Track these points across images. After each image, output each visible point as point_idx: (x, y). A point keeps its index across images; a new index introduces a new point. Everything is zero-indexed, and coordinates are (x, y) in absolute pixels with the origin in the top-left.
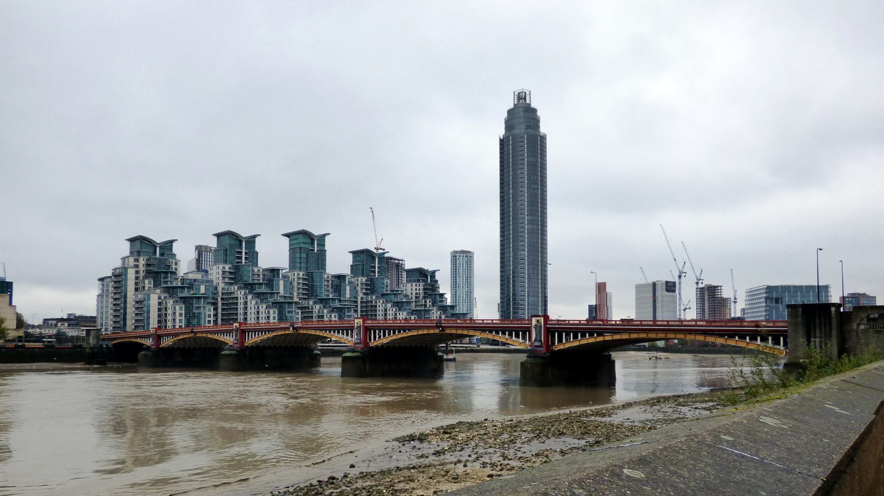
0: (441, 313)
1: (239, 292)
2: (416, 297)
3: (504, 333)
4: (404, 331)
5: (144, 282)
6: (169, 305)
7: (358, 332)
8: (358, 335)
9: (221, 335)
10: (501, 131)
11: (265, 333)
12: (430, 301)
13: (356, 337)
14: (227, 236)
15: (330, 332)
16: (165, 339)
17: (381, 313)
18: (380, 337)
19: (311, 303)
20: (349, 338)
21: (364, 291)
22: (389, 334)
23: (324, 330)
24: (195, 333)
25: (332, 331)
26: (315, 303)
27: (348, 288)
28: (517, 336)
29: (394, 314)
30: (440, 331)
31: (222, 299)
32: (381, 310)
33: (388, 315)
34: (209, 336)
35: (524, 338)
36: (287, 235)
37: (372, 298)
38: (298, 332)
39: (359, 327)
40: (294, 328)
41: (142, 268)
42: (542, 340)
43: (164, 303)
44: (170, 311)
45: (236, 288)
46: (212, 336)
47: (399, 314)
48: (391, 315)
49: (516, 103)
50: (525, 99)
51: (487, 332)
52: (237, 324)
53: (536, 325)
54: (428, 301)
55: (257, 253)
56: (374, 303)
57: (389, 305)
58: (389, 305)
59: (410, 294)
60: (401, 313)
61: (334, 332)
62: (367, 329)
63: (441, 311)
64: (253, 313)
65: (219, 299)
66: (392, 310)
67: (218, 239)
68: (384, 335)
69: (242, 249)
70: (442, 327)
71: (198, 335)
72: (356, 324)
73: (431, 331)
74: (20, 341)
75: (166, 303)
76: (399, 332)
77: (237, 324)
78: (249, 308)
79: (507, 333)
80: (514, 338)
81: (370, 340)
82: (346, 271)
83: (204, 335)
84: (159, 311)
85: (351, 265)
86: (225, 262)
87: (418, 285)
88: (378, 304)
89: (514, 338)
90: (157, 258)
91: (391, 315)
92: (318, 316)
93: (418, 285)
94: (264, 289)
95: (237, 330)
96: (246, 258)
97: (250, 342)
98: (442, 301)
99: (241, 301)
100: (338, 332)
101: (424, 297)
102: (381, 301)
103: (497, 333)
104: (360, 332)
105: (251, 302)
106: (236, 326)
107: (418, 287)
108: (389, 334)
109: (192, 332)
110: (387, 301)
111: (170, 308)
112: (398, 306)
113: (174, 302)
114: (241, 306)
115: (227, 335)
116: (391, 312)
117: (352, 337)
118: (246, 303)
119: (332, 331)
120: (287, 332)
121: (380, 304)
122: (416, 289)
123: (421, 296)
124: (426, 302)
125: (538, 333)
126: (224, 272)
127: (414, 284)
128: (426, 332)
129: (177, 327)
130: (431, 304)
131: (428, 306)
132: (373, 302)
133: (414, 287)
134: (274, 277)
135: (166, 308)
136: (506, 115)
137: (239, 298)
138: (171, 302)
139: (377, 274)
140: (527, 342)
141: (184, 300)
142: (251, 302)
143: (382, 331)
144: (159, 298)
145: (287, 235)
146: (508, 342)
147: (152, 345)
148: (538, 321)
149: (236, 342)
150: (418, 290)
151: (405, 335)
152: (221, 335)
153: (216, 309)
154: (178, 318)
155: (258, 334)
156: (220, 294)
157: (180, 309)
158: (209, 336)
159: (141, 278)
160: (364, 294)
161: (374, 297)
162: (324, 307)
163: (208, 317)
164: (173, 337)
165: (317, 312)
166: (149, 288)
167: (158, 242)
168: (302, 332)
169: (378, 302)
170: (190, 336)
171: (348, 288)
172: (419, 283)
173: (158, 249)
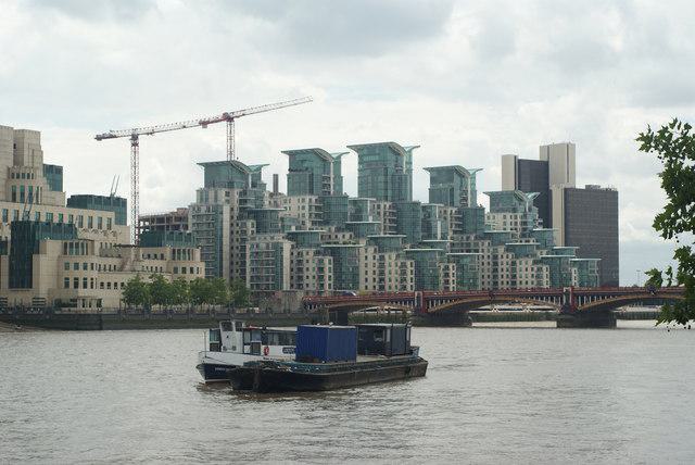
27: (439, 224)
37: (468, 238)
41: (236, 205)
57: (501, 250)
58: (501, 250)
64: (370, 265)
86: (311, 192)
101: (523, 236)
107: (513, 220)
116: (505, 259)
126: (310, 206)
127: (508, 215)
133: (508, 220)
138: (311, 254)
160: (455, 232)
166: (253, 232)
171: (439, 224)
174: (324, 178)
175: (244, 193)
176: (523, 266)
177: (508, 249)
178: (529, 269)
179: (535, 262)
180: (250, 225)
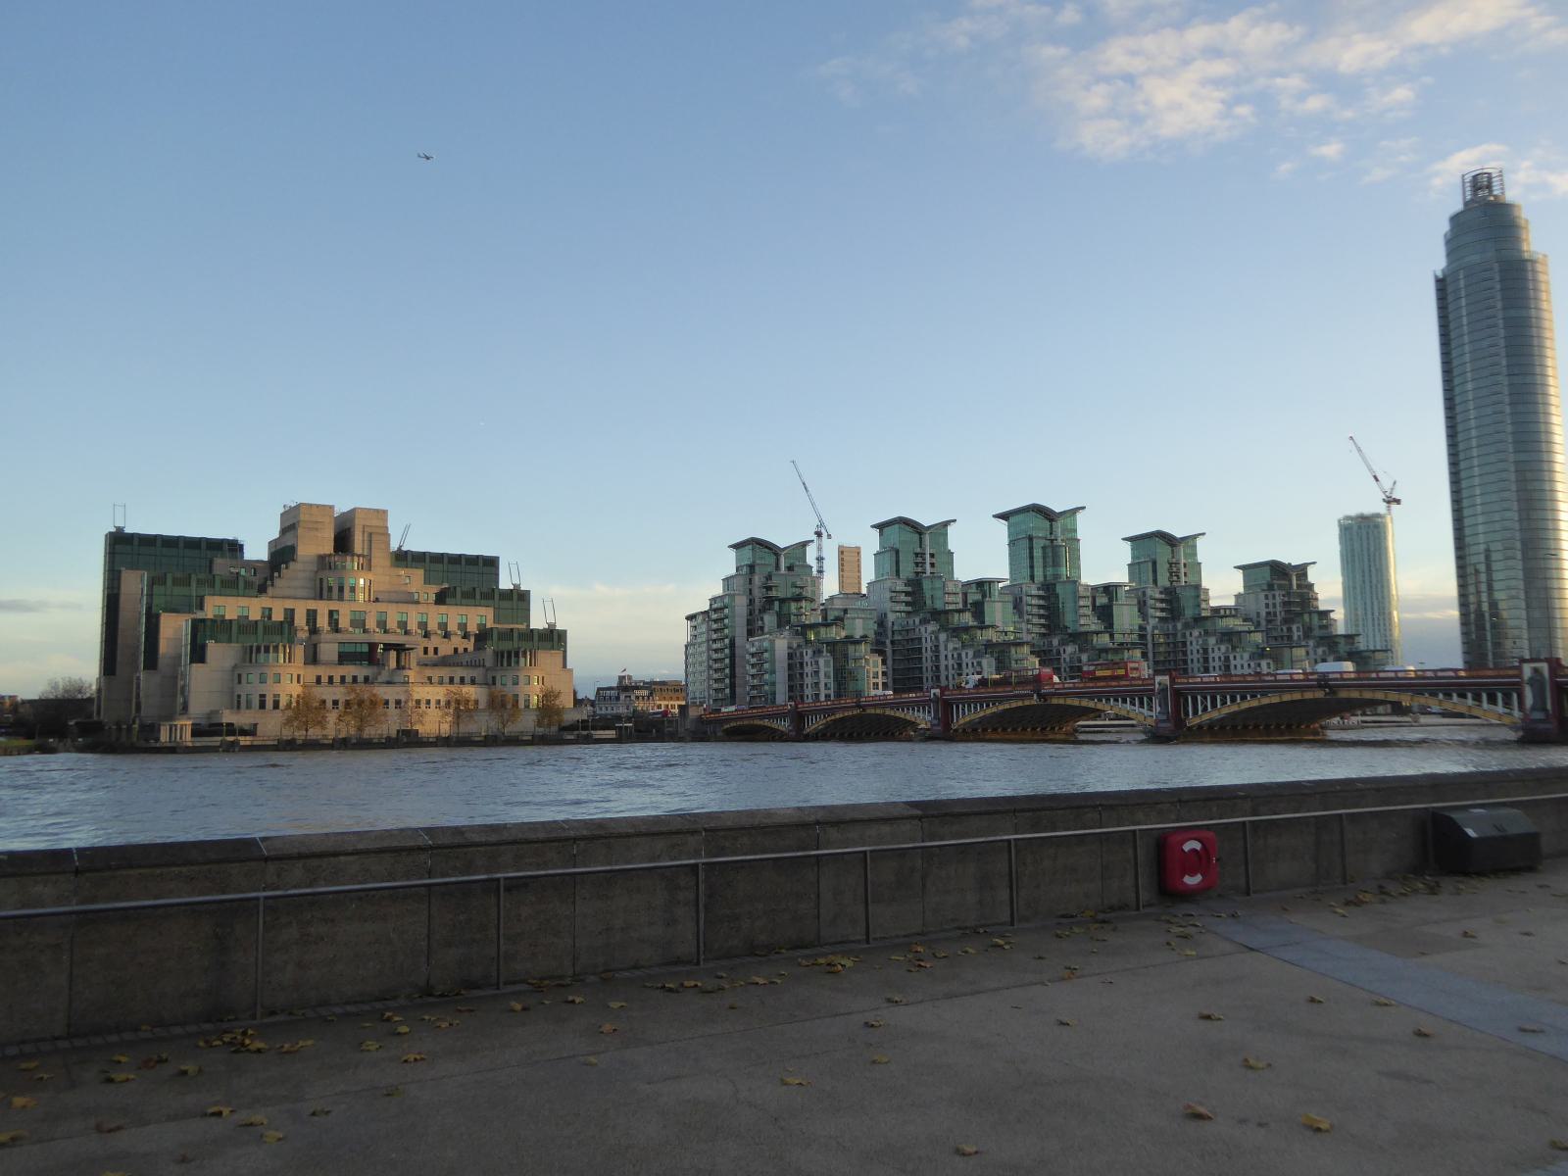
0: (1324, 652)
1: (923, 629)
2: (1269, 622)
3: (1463, 696)
4: (1253, 696)
5: (762, 619)
6: (807, 659)
7: (1162, 701)
8: (1163, 705)
9: (908, 709)
10: (1438, 262)
11: (988, 706)
12: (1298, 628)
13: (1158, 709)
14: (897, 526)
15: (1108, 700)
16: (812, 720)
17: (1195, 656)
18: (1205, 709)
19: (1055, 642)
20: (1145, 711)
21: (1158, 614)
22: (1224, 703)
23: (1096, 697)
24: (864, 708)
25: (1112, 700)
26: (1063, 643)
28: (1492, 700)
29: (1223, 659)
30: (1326, 694)
31: (892, 642)
32: (1195, 652)
33: (1211, 660)
34: (887, 713)
35: (1507, 703)
36: (1004, 516)
37: (1175, 627)
38: (1048, 702)
39: (1163, 690)
40: (1040, 696)
41: (758, 593)
42: (1549, 707)
43: (798, 654)
44: (808, 669)
45: (917, 621)
46: (892, 713)
47: (1235, 657)
48: (1217, 659)
49: (1469, 197)
50: (1489, 187)
51: (1427, 695)
52: (938, 691)
53: (1531, 679)
54: (1294, 628)
55: (951, 554)
56: (1179, 638)
57: (1212, 641)
58: (1212, 641)
59: (1254, 616)
60: (1238, 657)
61: (1116, 700)
62: (1179, 695)
63: (1325, 648)
65: (888, 642)
66: (1219, 649)
67: (881, 534)
68: (1214, 705)
69: (924, 550)
70: (1330, 687)
71: (868, 711)
72: (1157, 686)
73: (1309, 695)
74: (584, 729)
75: (802, 654)
76: (1243, 698)
77: (938, 691)
78: (942, 658)
79: (1469, 695)
80: (1485, 705)
81: (1187, 714)
82: (1121, 576)
83: (878, 711)
84: (789, 669)
85: (1129, 565)
87: (1270, 597)
88: (1189, 639)
89: (1485, 705)
90: (783, 575)
91: (1217, 659)
92: (1071, 668)
93: (1270, 597)
94: (967, 618)
95: (936, 700)
96: (932, 565)
97: (961, 722)
98: (1325, 627)
99: (927, 645)
100: (1124, 701)
101: (1286, 621)
102: (1196, 633)
103: (1448, 695)
104: (1166, 698)
105: (946, 647)
106: (934, 694)
108: (1224, 703)
109: (859, 706)
110: (1207, 633)
111: (809, 664)
112: (1230, 641)
113: (814, 652)
114: (927, 655)
115: (918, 711)
116: (1217, 654)
117: (1150, 709)
118: (937, 646)
119: (1112, 700)
120: (1027, 703)
121: (1193, 639)
122: (1267, 605)
123: (1279, 618)
124: (1289, 630)
125: (1539, 695)
128: (1297, 696)
129: (822, 698)
130: (1301, 633)
131: (1295, 638)
132: (1179, 635)
134: (984, 596)
135: (801, 664)
136: (1446, 227)
137: (924, 640)
138: (810, 652)
139: (1183, 579)
140: (1517, 713)
141: (832, 645)
142: (946, 647)
143: (1209, 698)
144: (789, 648)
145: (1004, 516)
146: (1475, 712)
147: (791, 731)
148: (1536, 670)
149: (936, 722)
150: (1271, 606)
151: (1255, 703)
152: (908, 709)
153: (884, 662)
154: (823, 680)
155: (975, 708)
156: (890, 634)
157: (825, 664)
158: (888, 712)
159: (757, 612)
161: (1179, 626)
162: (1081, 650)
163: (874, 678)
164: (824, 716)
165: (1068, 660)
167: (782, 545)
168: (1055, 701)
169: (1188, 634)
170: (855, 712)
172: (1273, 592)
173: (782, 559)
174: (917, 554)
175: (769, 577)
176: (1238, 662)
177: (1220, 641)
178: (1246, 666)
179: (1252, 657)
180: (769, 620)
